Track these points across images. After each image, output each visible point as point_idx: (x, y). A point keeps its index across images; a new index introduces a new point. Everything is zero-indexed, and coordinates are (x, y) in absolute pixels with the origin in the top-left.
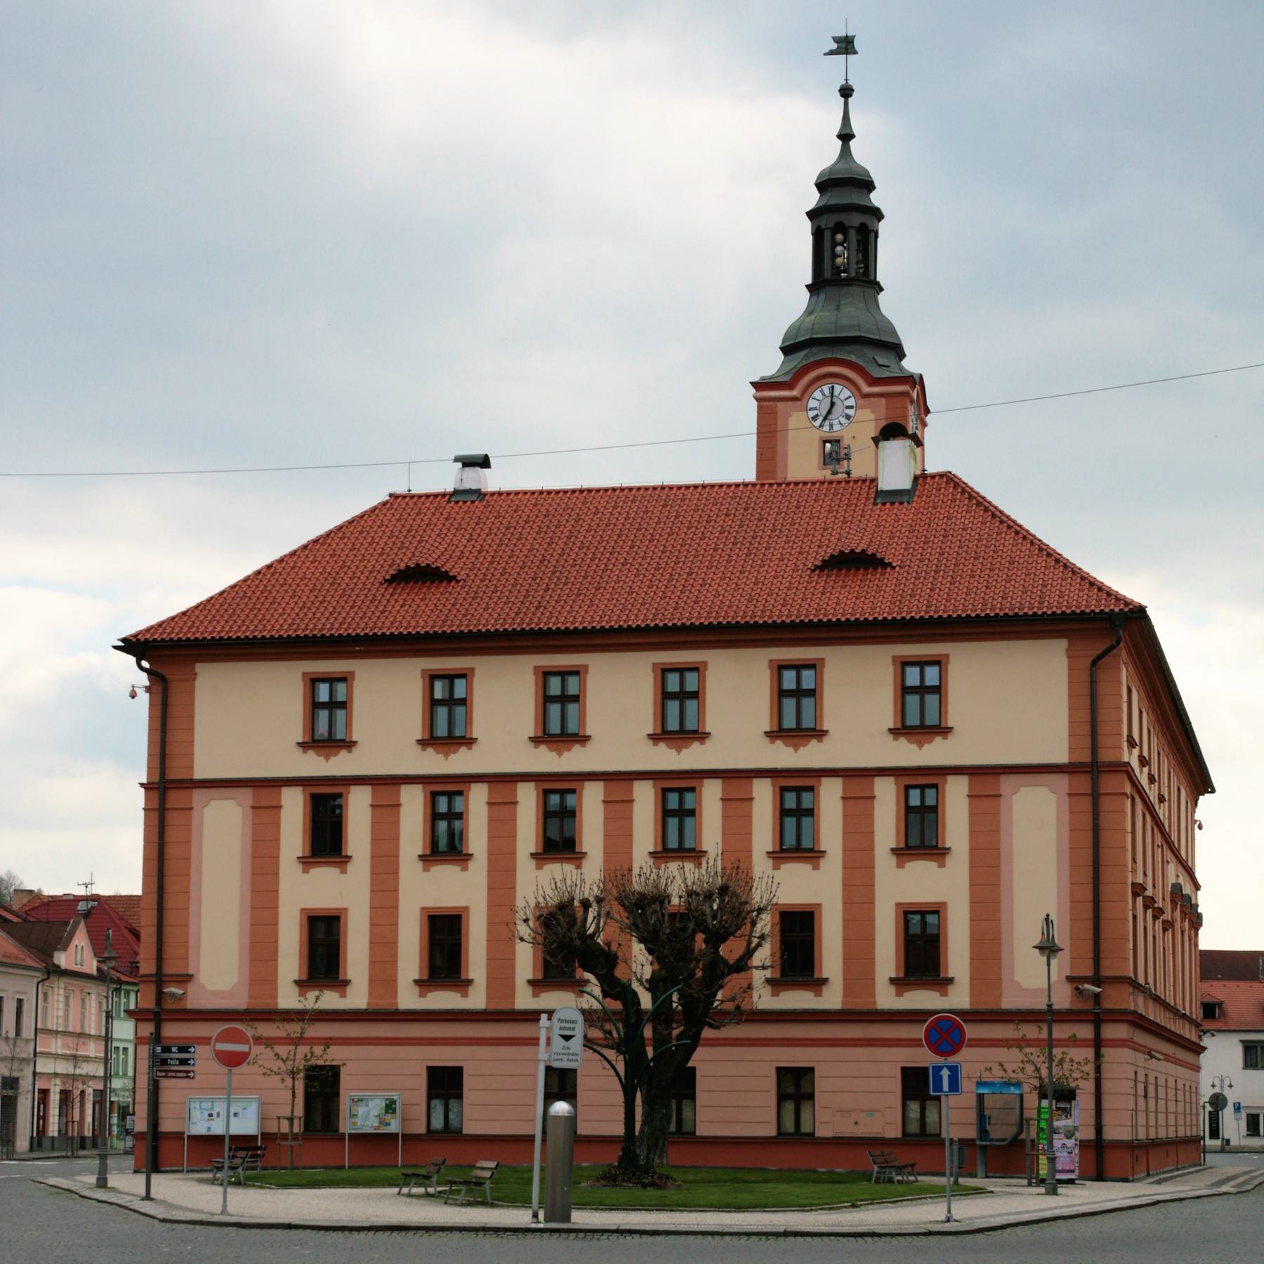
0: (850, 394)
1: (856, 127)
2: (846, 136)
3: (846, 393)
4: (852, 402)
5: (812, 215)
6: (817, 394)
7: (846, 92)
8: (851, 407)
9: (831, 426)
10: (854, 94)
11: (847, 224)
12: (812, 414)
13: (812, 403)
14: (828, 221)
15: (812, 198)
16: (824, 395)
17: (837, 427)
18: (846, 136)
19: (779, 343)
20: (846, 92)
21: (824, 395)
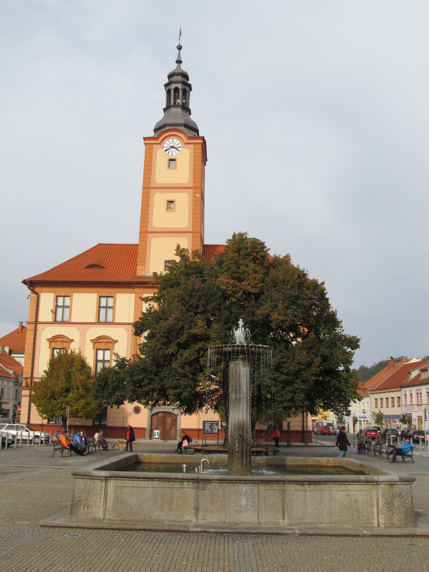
0: (179, 142)
1: (182, 59)
2: (179, 62)
3: (178, 142)
4: (180, 145)
5: (166, 86)
6: (167, 142)
7: (180, 48)
8: (180, 147)
9: (172, 154)
10: (182, 49)
11: (179, 88)
12: (165, 149)
13: (165, 145)
14: (173, 86)
15: (166, 81)
16: (170, 142)
17: (174, 154)
18: (179, 62)
19: (153, 128)
20: (180, 48)
21: (170, 142)
